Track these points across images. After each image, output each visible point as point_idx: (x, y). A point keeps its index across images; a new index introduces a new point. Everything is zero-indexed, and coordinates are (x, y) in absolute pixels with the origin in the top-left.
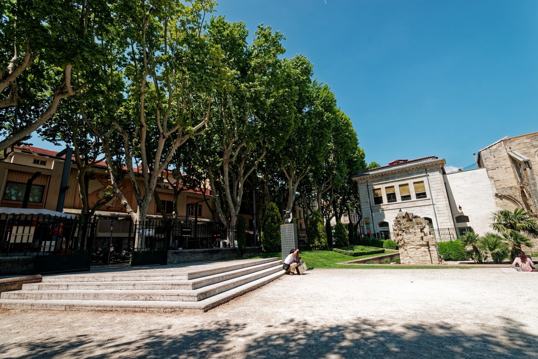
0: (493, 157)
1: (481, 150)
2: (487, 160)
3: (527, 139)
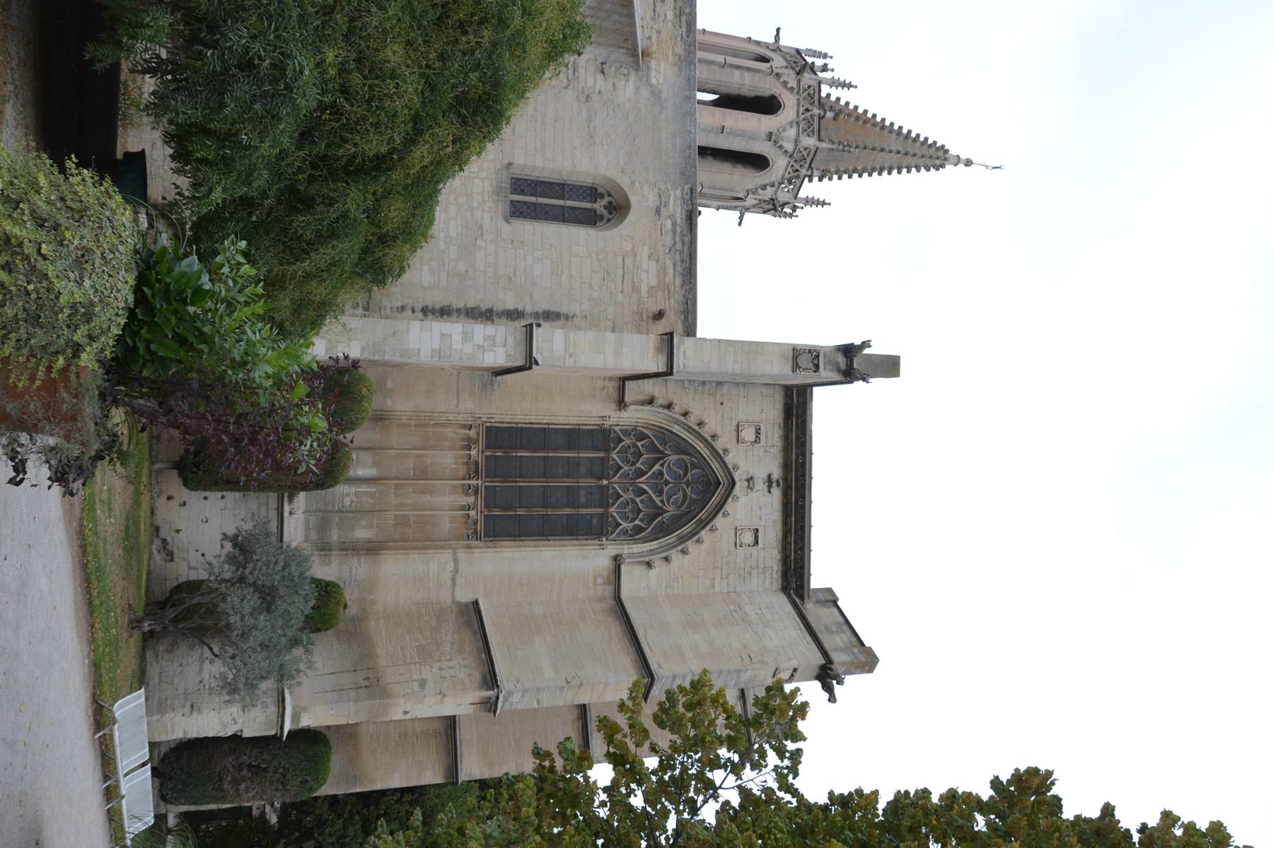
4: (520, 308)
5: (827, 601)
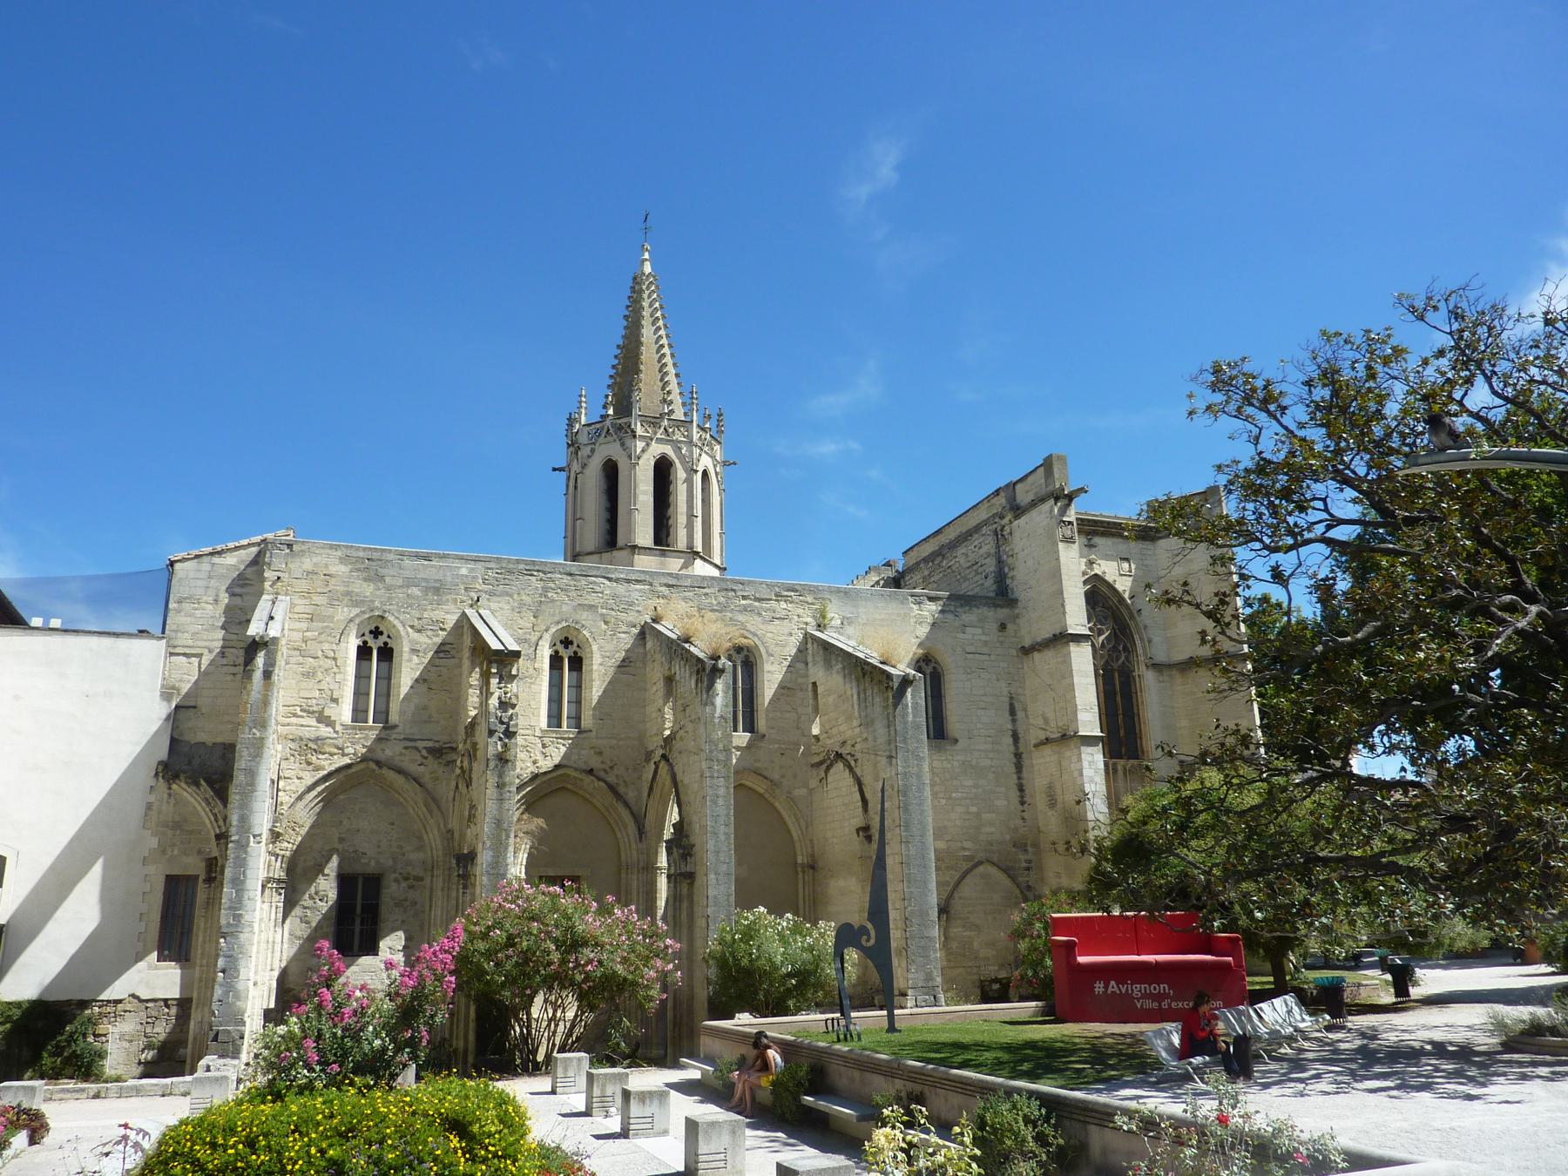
0: (210, 599)
1: (183, 555)
2: (187, 606)
3: (342, 561)
4: (1010, 733)
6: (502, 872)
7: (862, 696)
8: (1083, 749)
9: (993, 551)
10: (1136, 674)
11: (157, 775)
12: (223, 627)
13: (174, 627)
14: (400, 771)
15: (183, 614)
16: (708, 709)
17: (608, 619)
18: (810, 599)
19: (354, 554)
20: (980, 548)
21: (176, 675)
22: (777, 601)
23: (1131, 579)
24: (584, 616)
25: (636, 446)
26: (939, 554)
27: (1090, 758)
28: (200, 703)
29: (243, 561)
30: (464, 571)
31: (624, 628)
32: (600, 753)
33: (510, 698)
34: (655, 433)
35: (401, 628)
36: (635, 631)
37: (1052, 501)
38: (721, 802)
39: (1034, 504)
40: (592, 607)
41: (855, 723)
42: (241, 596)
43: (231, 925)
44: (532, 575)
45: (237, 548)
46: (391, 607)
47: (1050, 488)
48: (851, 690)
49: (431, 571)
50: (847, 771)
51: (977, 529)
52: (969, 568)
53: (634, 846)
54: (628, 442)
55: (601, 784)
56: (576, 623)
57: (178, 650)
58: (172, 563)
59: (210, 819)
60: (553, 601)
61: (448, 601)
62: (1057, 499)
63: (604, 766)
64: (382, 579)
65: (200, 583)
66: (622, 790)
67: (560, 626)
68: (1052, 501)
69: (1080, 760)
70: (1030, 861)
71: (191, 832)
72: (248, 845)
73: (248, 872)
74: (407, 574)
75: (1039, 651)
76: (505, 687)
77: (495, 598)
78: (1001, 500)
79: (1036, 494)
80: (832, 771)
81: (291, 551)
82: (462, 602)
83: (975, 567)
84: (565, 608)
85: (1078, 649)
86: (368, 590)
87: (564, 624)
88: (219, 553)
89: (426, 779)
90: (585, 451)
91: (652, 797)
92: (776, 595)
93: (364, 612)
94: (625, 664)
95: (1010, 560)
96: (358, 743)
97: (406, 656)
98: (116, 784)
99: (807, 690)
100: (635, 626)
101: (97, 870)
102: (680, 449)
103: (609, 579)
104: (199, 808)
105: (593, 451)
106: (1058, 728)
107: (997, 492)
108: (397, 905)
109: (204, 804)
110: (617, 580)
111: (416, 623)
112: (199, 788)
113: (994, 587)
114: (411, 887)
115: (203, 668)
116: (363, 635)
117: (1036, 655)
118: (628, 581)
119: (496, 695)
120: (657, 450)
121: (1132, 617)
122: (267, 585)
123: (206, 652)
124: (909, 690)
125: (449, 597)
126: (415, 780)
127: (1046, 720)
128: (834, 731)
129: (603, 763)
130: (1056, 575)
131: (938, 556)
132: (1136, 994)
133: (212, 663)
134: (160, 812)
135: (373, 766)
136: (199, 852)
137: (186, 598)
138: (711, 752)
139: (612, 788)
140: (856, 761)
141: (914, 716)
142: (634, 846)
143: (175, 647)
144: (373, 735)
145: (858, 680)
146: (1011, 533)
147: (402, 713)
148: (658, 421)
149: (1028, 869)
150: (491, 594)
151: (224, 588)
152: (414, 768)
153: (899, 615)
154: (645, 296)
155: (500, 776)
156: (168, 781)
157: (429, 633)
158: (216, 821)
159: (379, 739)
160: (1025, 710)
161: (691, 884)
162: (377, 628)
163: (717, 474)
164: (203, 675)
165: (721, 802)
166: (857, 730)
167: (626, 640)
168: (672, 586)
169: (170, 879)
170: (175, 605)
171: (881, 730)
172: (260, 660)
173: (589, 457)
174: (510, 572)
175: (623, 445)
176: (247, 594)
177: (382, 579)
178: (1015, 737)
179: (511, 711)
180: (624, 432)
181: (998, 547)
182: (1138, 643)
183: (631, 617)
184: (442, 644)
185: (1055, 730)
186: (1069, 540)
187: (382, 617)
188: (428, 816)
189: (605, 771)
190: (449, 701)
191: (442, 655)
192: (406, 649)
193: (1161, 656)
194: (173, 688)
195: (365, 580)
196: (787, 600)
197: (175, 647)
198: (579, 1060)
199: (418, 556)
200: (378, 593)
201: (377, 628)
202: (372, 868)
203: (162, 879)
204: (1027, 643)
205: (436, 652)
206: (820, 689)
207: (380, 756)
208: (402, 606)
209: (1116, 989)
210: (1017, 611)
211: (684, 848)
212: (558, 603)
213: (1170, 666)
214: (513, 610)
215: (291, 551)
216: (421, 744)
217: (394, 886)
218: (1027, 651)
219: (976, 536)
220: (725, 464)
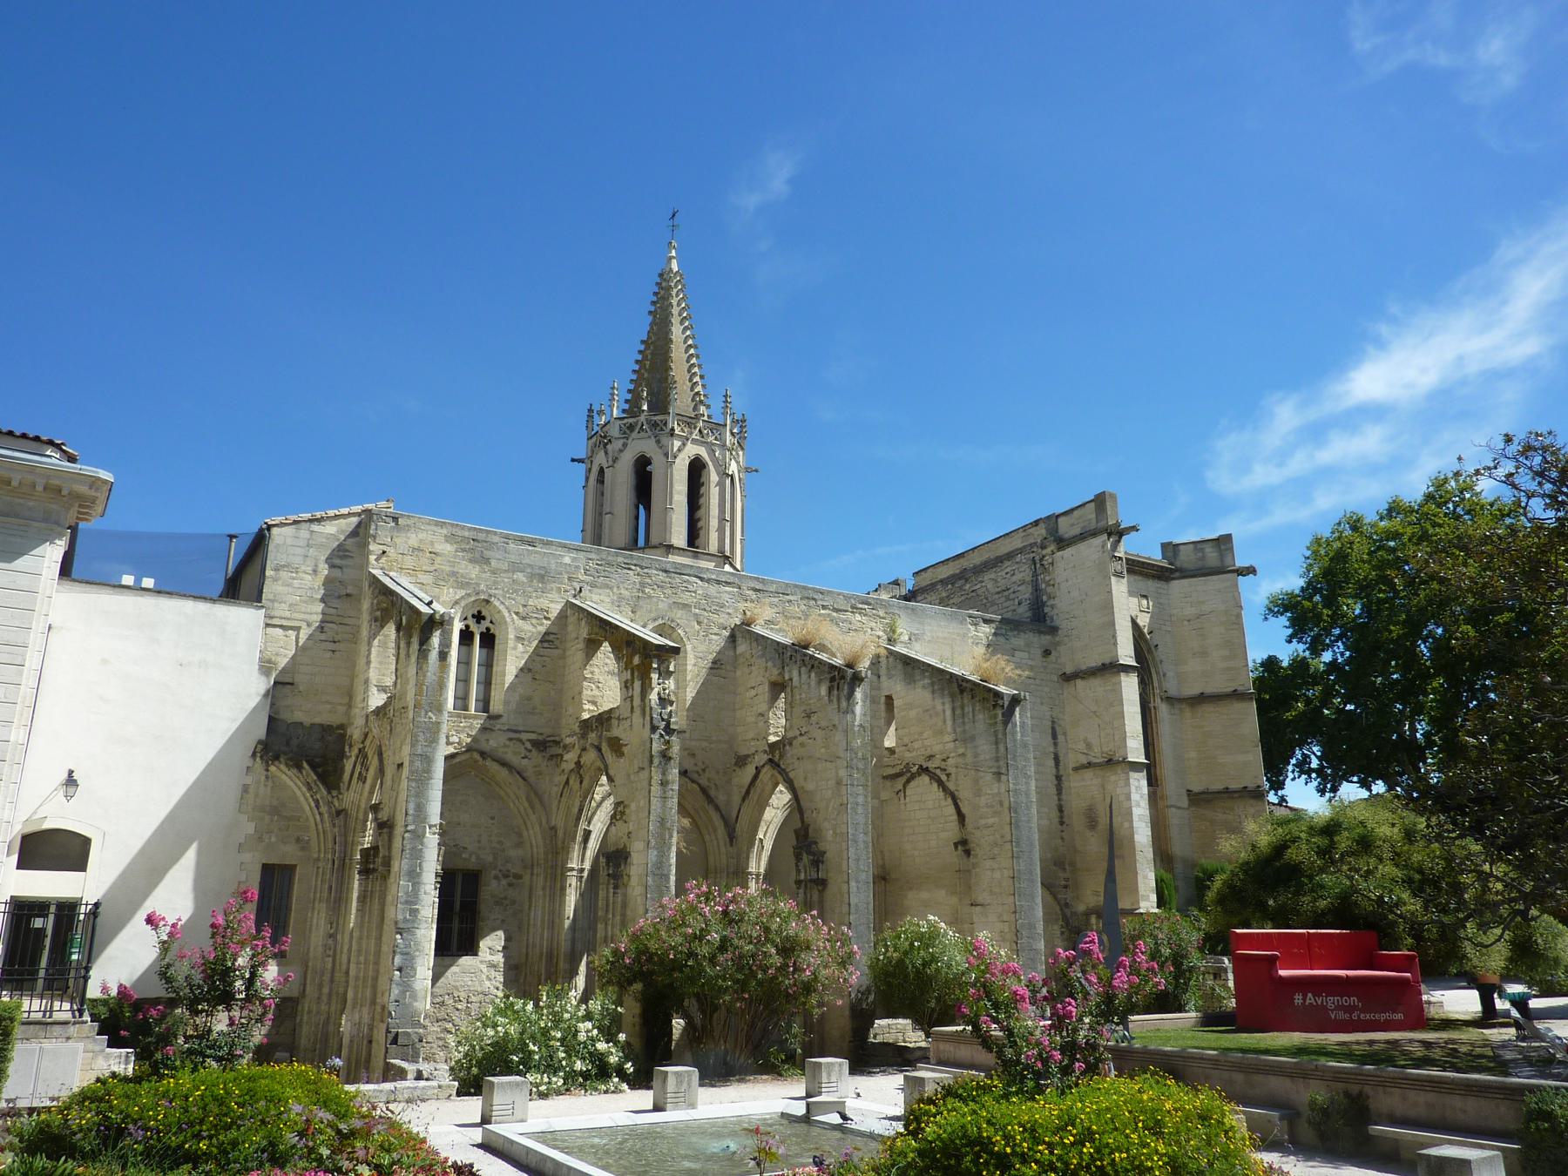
0: (309, 569)
2: (284, 574)
5: (1174, 551)
6: (666, 872)
7: (958, 712)
8: (1131, 774)
9: (1029, 579)
10: (1152, 705)
11: (254, 755)
12: (322, 600)
13: (271, 597)
14: (504, 764)
15: (280, 582)
16: (849, 717)
17: (701, 619)
18: (881, 613)
19: (460, 533)
20: (1013, 574)
21: (272, 649)
22: (852, 612)
23: (1149, 615)
24: (679, 614)
25: (673, 444)
26: (962, 576)
27: (1136, 783)
28: (297, 680)
29: (343, 531)
30: (567, 560)
31: (716, 630)
32: (693, 755)
33: (669, 695)
34: (691, 433)
35: (506, 614)
36: (726, 633)
37: (1105, 536)
38: (860, 810)
39: (1082, 537)
40: (685, 606)
41: (948, 738)
42: (340, 568)
43: (408, 920)
44: (629, 569)
45: (336, 517)
46: (496, 592)
47: (1102, 524)
48: (943, 706)
49: (535, 557)
50: (935, 785)
51: (1010, 556)
52: (998, 593)
53: (723, 849)
54: (664, 440)
55: (695, 786)
56: (672, 621)
57: (275, 621)
58: (269, 527)
59: (310, 806)
60: (650, 597)
61: (552, 590)
62: (1110, 535)
63: (696, 769)
64: (487, 561)
65: (299, 551)
66: (712, 793)
67: (657, 623)
68: (1105, 536)
69: (1128, 784)
70: (1067, 880)
71: (289, 819)
72: (424, 836)
73: (424, 865)
74: (513, 558)
75: (1083, 678)
76: (664, 683)
77: (595, 590)
78: (1041, 531)
79: (1082, 528)
80: (913, 784)
81: (397, 524)
82: (566, 591)
83: (1006, 593)
84: (661, 606)
85: (1126, 679)
86: (473, 571)
87: (660, 622)
88: (319, 520)
89: (529, 774)
90: (618, 444)
91: (747, 801)
92: (852, 607)
93: (469, 595)
94: (716, 665)
95: (1050, 589)
96: (463, 731)
97: (511, 643)
98: (210, 764)
99: (879, 703)
100: (725, 628)
101: (190, 856)
102: (714, 451)
103: (701, 579)
104: (299, 793)
105: (625, 445)
106: (1102, 753)
107: (1036, 523)
108: (497, 903)
109: (304, 789)
110: (708, 581)
111: (521, 610)
112: (301, 773)
113: (1029, 614)
114: (510, 885)
115: (300, 644)
116: (465, 619)
117: (1079, 682)
118: (719, 582)
119: (656, 690)
120: (692, 450)
121: (1150, 651)
122: (372, 558)
123: (304, 625)
124: (1017, 709)
125: (553, 585)
126: (518, 773)
127: (1089, 746)
128: (916, 745)
129: (696, 765)
130: (1108, 606)
131: (960, 579)
132: (1331, 1006)
133: (310, 637)
134: (257, 795)
135: (476, 756)
136: (298, 840)
137: (284, 566)
138: (851, 760)
139: (704, 791)
140: (948, 775)
141: (1022, 736)
142: (723, 849)
143: (272, 618)
144: (477, 724)
145: (952, 696)
146: (1052, 564)
147: (506, 703)
148: (694, 421)
149: (1066, 887)
150: (593, 585)
151: (323, 558)
152: (515, 760)
153: (958, 635)
154: (674, 292)
155: (664, 774)
156: (267, 762)
157: (534, 621)
158: (318, 807)
159: (484, 729)
160: (1065, 734)
161: (821, 892)
162: (479, 612)
163: (740, 479)
164: (301, 650)
165: (860, 810)
166: (951, 745)
167: (718, 641)
168: (759, 590)
169: (268, 870)
170: (272, 573)
171: (985, 748)
172: (436, 640)
173: (621, 451)
174: (610, 564)
175: (658, 442)
176: (347, 566)
177: (487, 561)
178: (1057, 759)
179: (669, 708)
180: (659, 429)
181: (1035, 575)
182: (1154, 676)
183: (722, 619)
184: (546, 633)
185: (1099, 755)
186: (1119, 575)
187: (487, 602)
188: (530, 811)
189: (698, 772)
190: (553, 693)
191: (546, 645)
192: (511, 636)
193: (1173, 692)
194: (269, 661)
195: (471, 561)
196: (861, 612)
197: (272, 618)
198: (840, 1065)
199: (522, 541)
200: (484, 575)
201: (479, 612)
202: (472, 864)
203: (258, 868)
204: (1069, 670)
205: (541, 641)
206: (896, 703)
207: (485, 747)
208: (508, 591)
209: (1313, 1000)
210: (1057, 639)
211: (814, 854)
212: (655, 600)
213: (1180, 700)
214: (612, 603)
215: (397, 524)
216: (524, 736)
217: (494, 883)
218: (1068, 678)
219: (1007, 563)
220: (748, 470)
